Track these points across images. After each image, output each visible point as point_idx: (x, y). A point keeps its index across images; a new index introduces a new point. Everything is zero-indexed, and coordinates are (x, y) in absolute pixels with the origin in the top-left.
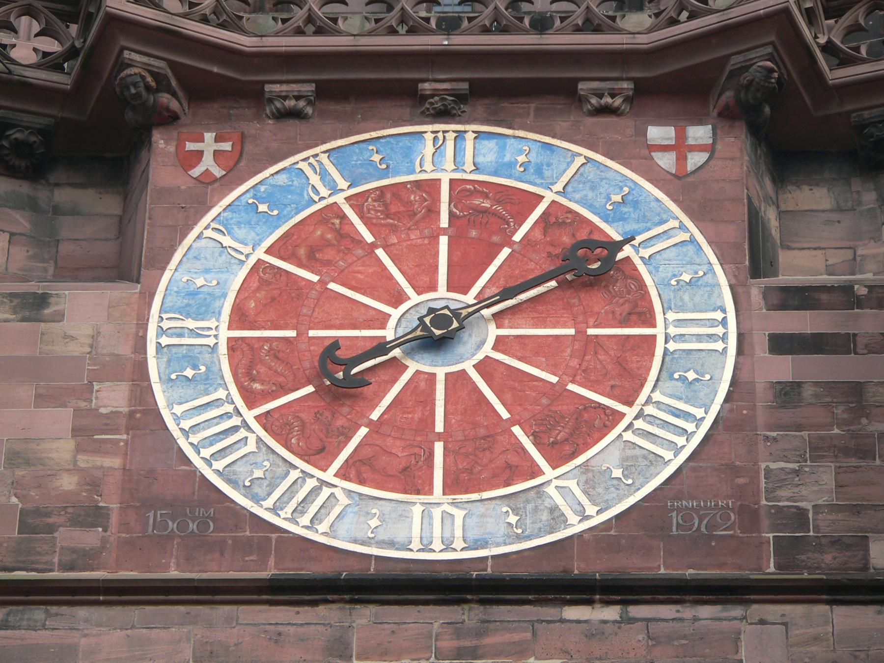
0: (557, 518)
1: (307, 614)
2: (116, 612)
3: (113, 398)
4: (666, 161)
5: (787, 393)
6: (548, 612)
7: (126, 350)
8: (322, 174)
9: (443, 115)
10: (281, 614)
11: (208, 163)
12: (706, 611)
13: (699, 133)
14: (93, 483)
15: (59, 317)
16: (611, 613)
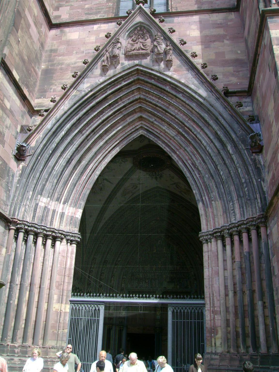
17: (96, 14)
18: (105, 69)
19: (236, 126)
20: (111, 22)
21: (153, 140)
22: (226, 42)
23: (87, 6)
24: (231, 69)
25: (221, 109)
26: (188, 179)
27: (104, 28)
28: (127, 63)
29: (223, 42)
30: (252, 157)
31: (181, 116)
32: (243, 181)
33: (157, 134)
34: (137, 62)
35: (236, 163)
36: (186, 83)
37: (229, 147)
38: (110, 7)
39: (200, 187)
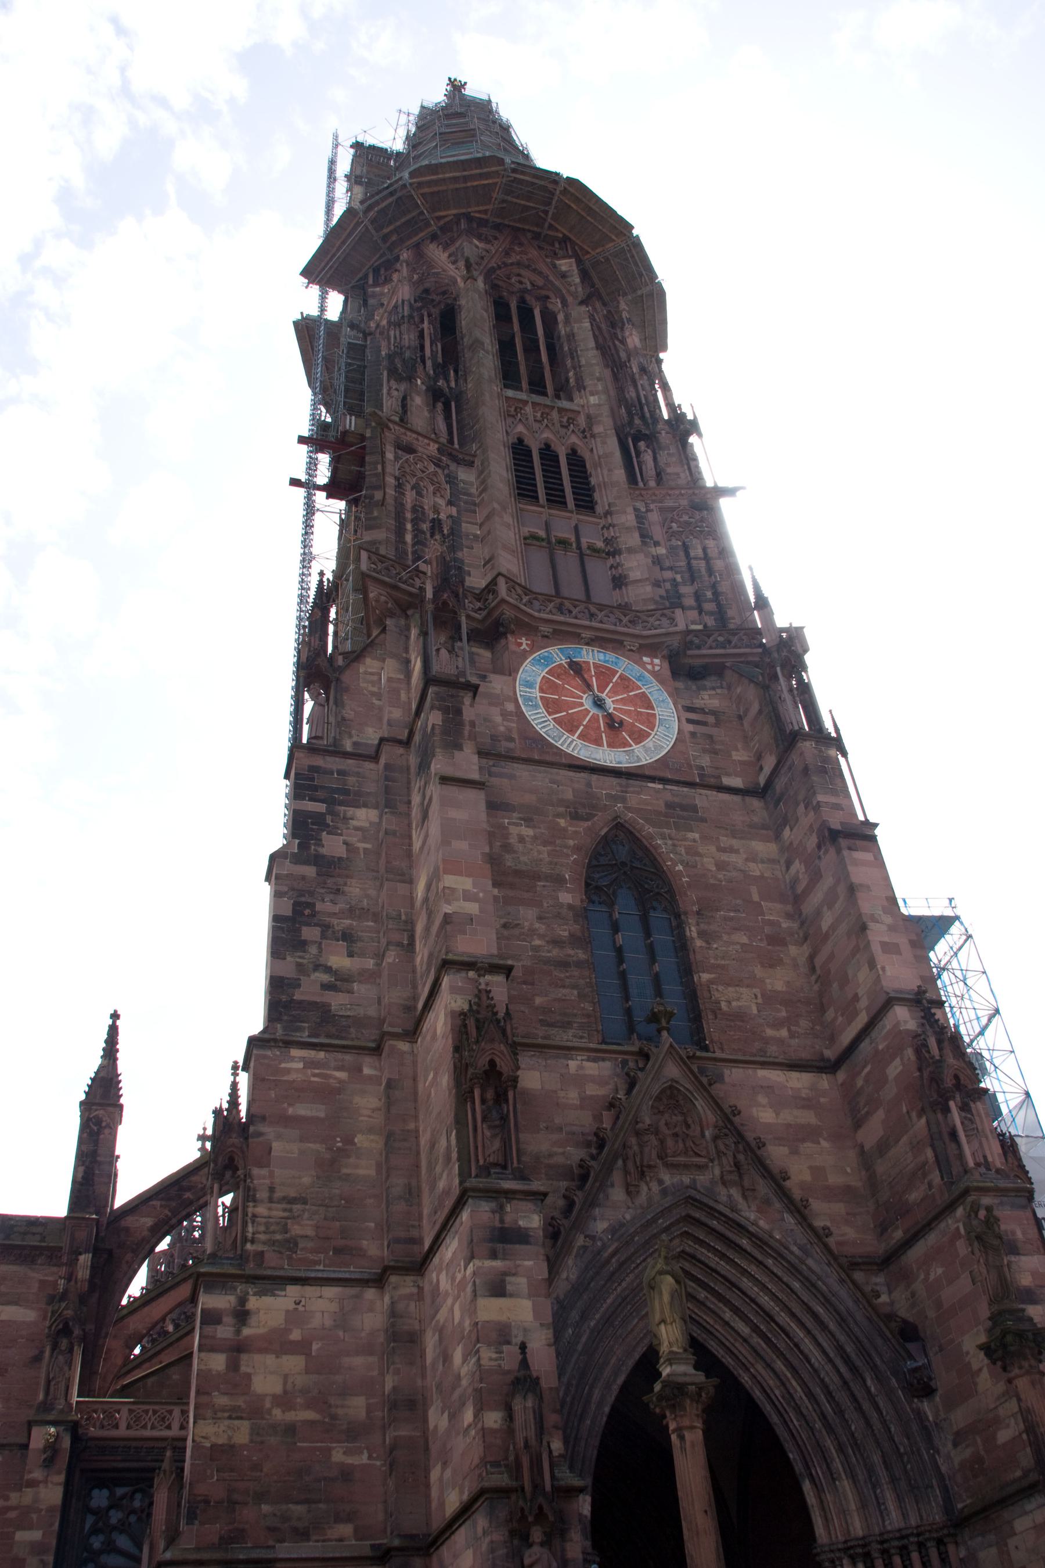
0: (639, 760)
1: (578, 775)
2: (524, 766)
3: (510, 707)
4: (649, 667)
5: (693, 734)
6: (644, 784)
7: (511, 694)
8: (557, 655)
9: (587, 644)
10: (571, 774)
11: (524, 646)
12: (685, 789)
13: (657, 661)
14: (509, 730)
15: (490, 682)
16: (661, 786)
17: (566, 1025)
18: (631, 1191)
19: (879, 1341)
20: (603, 1060)
21: (699, 1338)
22: (825, 1144)
23: (538, 1001)
24: (839, 1208)
25: (850, 1304)
26: (776, 1428)
27: (591, 1072)
28: (667, 1178)
29: (819, 1143)
30: (914, 1406)
31: (765, 1300)
32: (902, 1450)
33: (708, 1327)
34: (686, 1180)
35: (884, 1413)
36: (784, 1240)
37: (869, 1382)
38: (588, 1016)
39: (803, 1448)
